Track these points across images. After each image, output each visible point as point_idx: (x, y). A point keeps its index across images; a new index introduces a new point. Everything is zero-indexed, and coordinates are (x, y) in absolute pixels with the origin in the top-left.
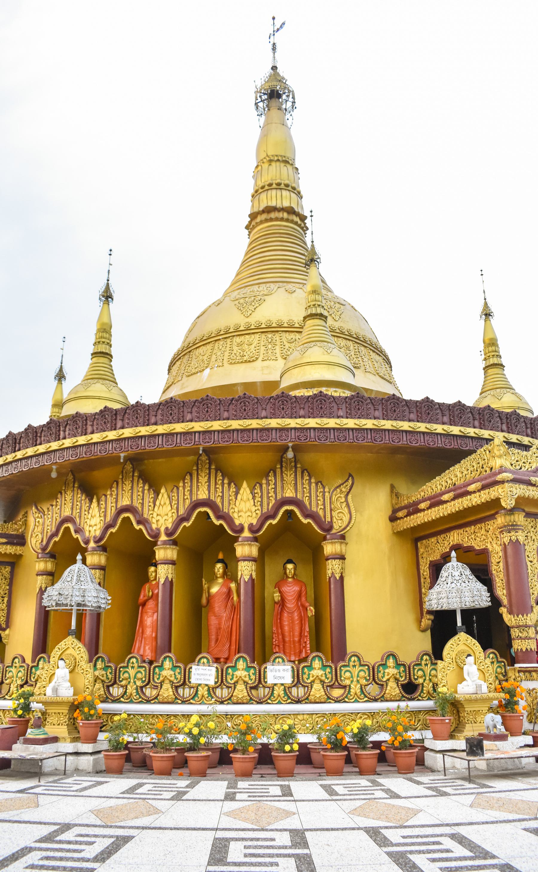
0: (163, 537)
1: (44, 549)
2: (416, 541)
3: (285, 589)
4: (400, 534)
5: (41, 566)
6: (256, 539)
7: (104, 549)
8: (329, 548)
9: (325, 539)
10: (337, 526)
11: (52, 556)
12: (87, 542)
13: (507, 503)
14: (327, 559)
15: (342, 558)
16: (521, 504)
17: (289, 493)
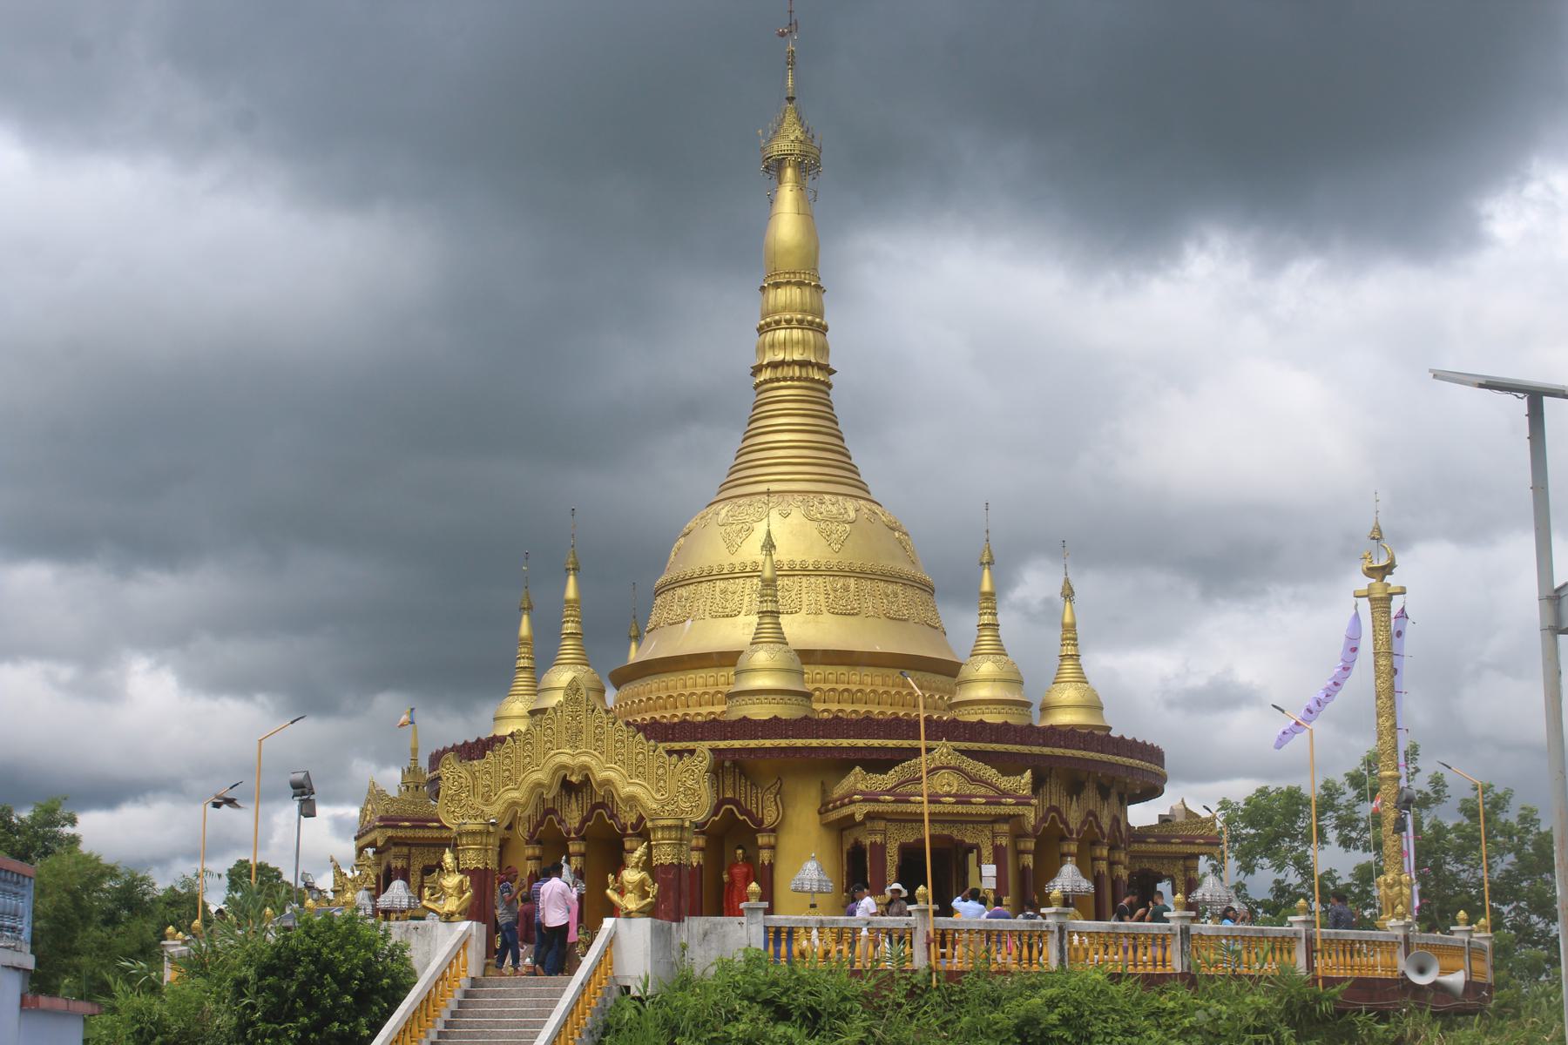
0: (630, 831)
1: (531, 837)
2: (843, 830)
3: (736, 870)
4: (828, 826)
5: (529, 851)
6: (703, 833)
7: (583, 839)
8: (762, 840)
9: (759, 831)
10: (768, 821)
11: (539, 842)
12: (569, 833)
13: (859, 817)
14: (761, 848)
15: (772, 847)
16: (870, 816)
17: (729, 795)
